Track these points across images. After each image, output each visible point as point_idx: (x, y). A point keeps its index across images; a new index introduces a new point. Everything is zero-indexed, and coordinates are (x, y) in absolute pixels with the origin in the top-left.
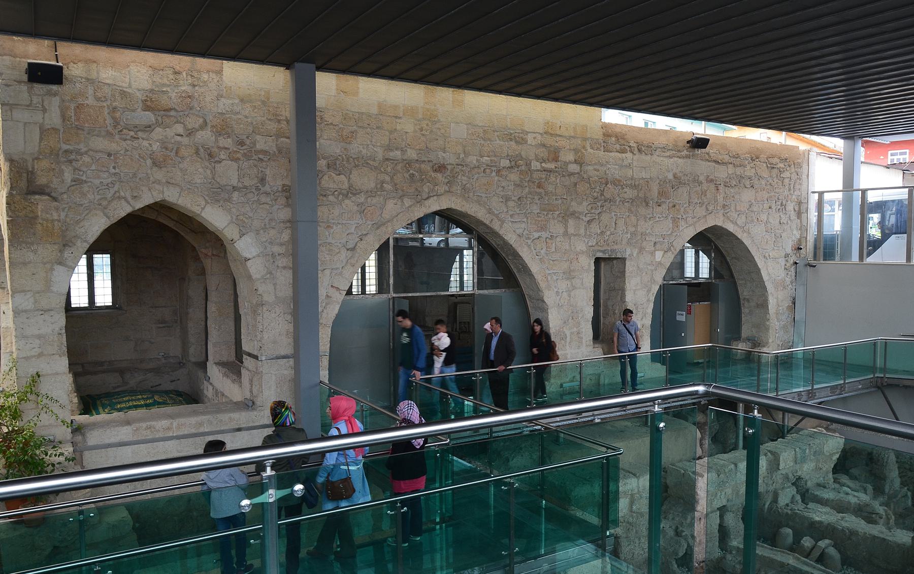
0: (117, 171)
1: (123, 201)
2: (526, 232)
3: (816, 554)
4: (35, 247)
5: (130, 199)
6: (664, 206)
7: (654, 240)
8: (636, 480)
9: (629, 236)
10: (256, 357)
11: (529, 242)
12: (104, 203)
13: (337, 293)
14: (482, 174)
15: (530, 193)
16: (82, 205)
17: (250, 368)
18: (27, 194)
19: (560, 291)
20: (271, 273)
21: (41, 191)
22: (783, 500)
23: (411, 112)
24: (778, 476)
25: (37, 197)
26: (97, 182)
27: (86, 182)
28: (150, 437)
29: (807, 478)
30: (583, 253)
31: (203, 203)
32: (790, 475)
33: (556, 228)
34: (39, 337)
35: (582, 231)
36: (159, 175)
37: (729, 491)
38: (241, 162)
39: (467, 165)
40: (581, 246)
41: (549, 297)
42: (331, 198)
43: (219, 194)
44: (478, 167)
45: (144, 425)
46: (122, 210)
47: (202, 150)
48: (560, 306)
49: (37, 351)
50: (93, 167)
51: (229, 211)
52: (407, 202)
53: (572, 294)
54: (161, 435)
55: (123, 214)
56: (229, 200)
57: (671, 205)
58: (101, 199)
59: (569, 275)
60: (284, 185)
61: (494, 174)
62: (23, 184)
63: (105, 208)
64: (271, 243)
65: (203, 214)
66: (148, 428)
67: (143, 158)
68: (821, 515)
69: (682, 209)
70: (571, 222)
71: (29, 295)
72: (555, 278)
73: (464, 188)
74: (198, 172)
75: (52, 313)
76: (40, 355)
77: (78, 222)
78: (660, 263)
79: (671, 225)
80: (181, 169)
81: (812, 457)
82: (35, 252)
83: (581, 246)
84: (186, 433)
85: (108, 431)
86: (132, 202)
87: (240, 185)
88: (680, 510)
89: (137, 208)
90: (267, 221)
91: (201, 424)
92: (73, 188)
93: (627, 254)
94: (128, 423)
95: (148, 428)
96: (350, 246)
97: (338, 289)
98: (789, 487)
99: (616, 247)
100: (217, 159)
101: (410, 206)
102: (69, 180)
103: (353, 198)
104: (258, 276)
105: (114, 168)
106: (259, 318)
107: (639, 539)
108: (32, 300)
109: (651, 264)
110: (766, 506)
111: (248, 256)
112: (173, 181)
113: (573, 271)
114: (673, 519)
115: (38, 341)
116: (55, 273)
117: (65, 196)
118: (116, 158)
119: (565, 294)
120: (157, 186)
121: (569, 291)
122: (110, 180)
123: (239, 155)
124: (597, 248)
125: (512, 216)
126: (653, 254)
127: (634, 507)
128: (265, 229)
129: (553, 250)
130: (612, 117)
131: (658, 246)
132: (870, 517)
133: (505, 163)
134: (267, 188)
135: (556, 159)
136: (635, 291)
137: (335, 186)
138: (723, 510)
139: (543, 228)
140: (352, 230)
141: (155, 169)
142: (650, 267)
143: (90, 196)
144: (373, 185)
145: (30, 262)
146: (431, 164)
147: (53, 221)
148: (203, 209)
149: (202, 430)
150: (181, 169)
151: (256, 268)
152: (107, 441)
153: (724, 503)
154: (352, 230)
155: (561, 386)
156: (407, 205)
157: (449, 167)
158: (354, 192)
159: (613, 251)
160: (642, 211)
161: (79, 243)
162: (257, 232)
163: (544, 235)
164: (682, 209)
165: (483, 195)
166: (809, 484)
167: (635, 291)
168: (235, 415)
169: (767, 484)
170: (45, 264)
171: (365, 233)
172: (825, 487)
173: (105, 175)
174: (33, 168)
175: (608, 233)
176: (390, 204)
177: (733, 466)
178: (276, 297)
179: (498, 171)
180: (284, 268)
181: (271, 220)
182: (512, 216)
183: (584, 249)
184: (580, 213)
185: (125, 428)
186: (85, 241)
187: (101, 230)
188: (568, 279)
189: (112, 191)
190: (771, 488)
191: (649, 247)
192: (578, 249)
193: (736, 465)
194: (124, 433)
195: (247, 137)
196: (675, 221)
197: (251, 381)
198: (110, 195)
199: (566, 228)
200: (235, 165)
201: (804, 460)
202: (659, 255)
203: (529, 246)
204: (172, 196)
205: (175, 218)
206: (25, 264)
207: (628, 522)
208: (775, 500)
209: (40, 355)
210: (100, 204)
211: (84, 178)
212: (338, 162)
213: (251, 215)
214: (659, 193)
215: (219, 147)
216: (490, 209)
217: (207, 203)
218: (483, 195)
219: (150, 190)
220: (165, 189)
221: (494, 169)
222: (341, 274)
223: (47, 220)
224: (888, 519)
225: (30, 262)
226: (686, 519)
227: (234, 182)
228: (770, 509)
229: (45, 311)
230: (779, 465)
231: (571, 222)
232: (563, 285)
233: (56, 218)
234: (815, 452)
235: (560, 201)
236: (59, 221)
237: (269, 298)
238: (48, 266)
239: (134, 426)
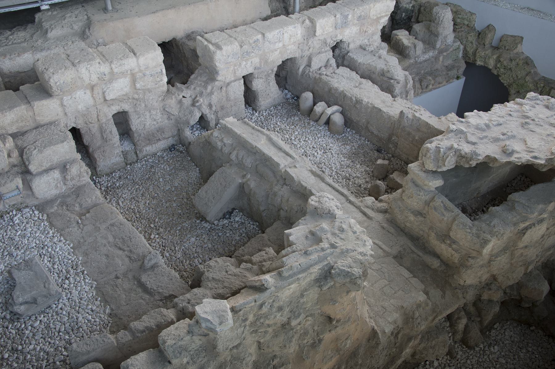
3: (324, 119)
8: (135, 59)
22: (316, 64)
24: (315, 43)
29: (349, 41)
32: (329, 41)
68: (344, 81)
81: (356, 22)
88: (205, 79)
107: (150, 112)
110: (301, 70)
114: (195, 89)
127: (138, 86)
132: (385, 83)
153: (250, 70)
166: (352, 46)
169: (302, 50)
172: (365, 49)
177: (260, 36)
190: (307, 53)
193: (263, 35)
201: (345, 24)
207: (134, 99)
208: (309, 65)
224: (407, 83)
226: (206, 89)
228: (304, 72)
230: (315, 31)
234: (360, 17)
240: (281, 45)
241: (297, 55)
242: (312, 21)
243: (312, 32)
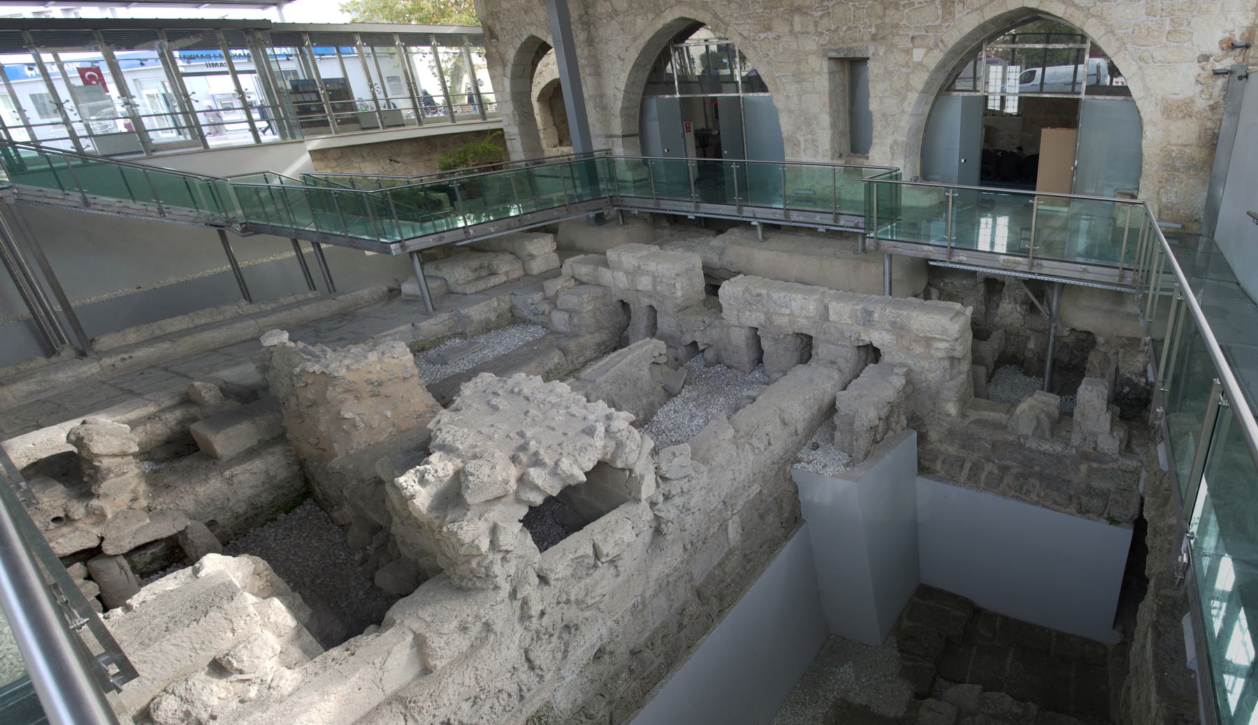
7: (911, 33)
9: (873, 30)
33: (780, 27)
35: (811, 28)
40: (811, 44)
59: (798, 78)
70: (797, 19)
78: (920, 64)
79: (940, 12)
83: (811, 44)
99: (854, 45)
109: (907, 65)
121: (799, 96)
126: (908, 52)
131: (917, 42)
139: (768, 28)
142: (904, 70)
159: (850, 49)
163: (771, 35)
175: (845, 28)
176: (639, 20)
183: (815, 47)
184: (810, 7)
188: (798, 82)
191: (904, 43)
192: (808, 48)
199: (792, 25)
202: (918, 55)
203: (755, 48)
231: (797, 19)
232: (792, 88)
240: (788, 312)
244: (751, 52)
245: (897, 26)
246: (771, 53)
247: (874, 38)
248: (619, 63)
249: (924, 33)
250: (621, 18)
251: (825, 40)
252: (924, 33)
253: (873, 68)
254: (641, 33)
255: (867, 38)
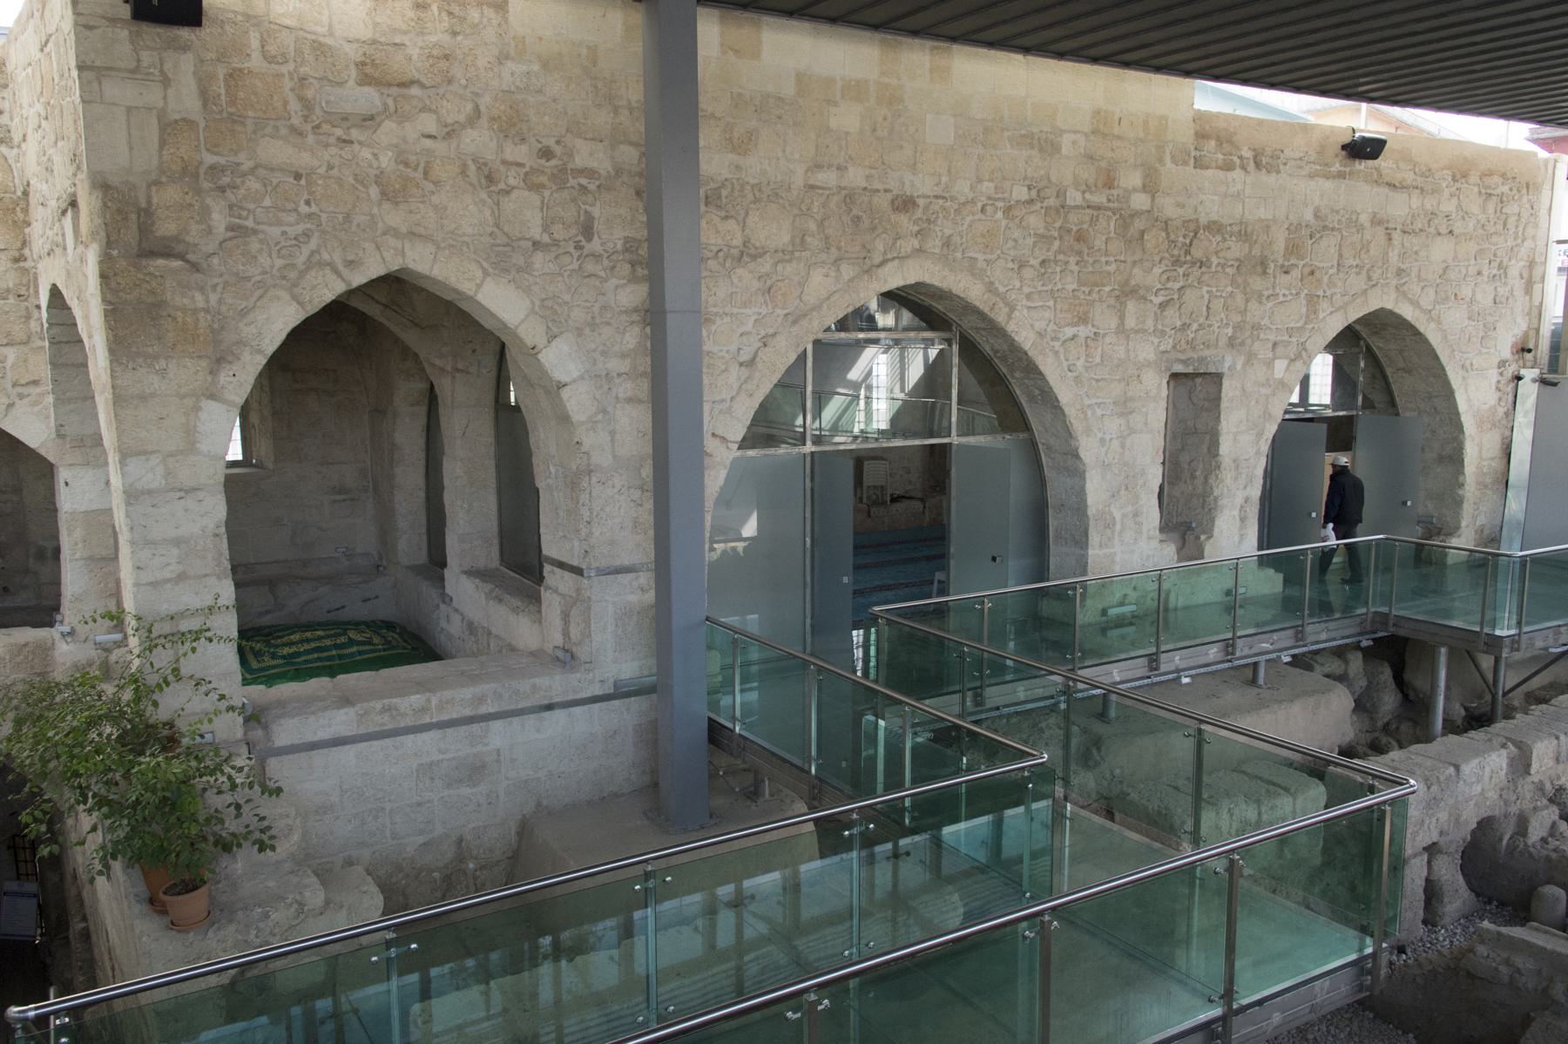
0: (314, 209)
1: (327, 270)
2: (1052, 326)
4: (163, 363)
5: (341, 268)
6: (1296, 273)
7: (1272, 337)
10: (578, 571)
11: (1057, 344)
12: (293, 275)
13: (723, 449)
14: (979, 216)
15: (1060, 251)
16: (248, 279)
17: (562, 589)
18: (138, 256)
19: (1108, 437)
20: (605, 411)
21: (166, 250)
22: (1537, 831)
23: (856, 90)
24: (1526, 788)
25: (161, 262)
26: (275, 232)
27: (255, 232)
28: (390, 726)
30: (1149, 365)
31: (479, 274)
32: (1548, 786)
33: (1105, 319)
34: (178, 542)
35: (1150, 323)
36: (394, 217)
37: (1443, 816)
38: (547, 193)
39: (953, 199)
41: (1089, 450)
42: (712, 264)
43: (504, 255)
44: (973, 201)
45: (378, 705)
46: (326, 290)
47: (473, 167)
48: (1106, 467)
49: (175, 569)
50: (267, 202)
51: (527, 291)
52: (847, 271)
53: (1128, 443)
54: (409, 722)
55: (329, 297)
56: (527, 268)
57: (1307, 270)
58: (286, 266)
59: (1124, 406)
60: (627, 240)
61: (1000, 215)
62: (131, 235)
63: (295, 285)
64: (604, 353)
65: (480, 297)
66: (385, 710)
67: (362, 183)
69: (1326, 279)
70: (1131, 306)
71: (155, 460)
72: (1099, 412)
73: (947, 243)
74: (468, 213)
75: (201, 495)
76: (181, 577)
77: (243, 313)
80: (435, 207)
82: (163, 373)
83: (1146, 351)
84: (455, 716)
85: (312, 718)
86: (345, 272)
87: (546, 239)
89: (355, 284)
90: (596, 310)
91: (481, 700)
92: (229, 244)
93: (1227, 365)
94: (346, 701)
95: (385, 710)
96: (745, 357)
97: (723, 439)
98: (1546, 807)
99: (1206, 353)
100: (502, 186)
101: (852, 280)
102: (222, 229)
103: (752, 266)
104: (583, 418)
105: (308, 203)
106: (584, 497)
108: (160, 470)
111: (564, 378)
112: (421, 231)
113: (1132, 399)
115: (175, 551)
116: (203, 415)
117: (215, 261)
118: (309, 184)
119: (1116, 443)
120: (392, 242)
122: (300, 228)
123: (543, 179)
124: (1174, 355)
125: (1028, 296)
126: (1270, 364)
128: (593, 326)
129: (1098, 360)
130: (1215, 99)
131: (1279, 350)
133: (1020, 193)
134: (596, 245)
135: (1109, 184)
136: (1236, 435)
137: (720, 241)
138: (1432, 850)
139: (1083, 320)
140: (749, 327)
141: (386, 206)
142: (1264, 391)
143: (264, 260)
144: (786, 239)
145: (153, 395)
146: (889, 196)
147: (195, 311)
148: (479, 286)
149: (483, 710)
150: (435, 207)
151: (578, 402)
152: (310, 738)
153: (1435, 837)
154: (749, 327)
155: (1104, 612)
156: (846, 278)
157: (921, 202)
158: (752, 251)
159: (1202, 360)
160: (1257, 283)
161: (246, 356)
162: (579, 332)
163: (1083, 331)
164: (1326, 279)
165: (980, 257)
167: (1236, 435)
168: (542, 681)
169: (1506, 803)
170: (182, 397)
171: (771, 331)
173: (292, 218)
174: (149, 202)
175: (1195, 326)
177: (1452, 769)
178: (615, 457)
179: (1008, 210)
180: (629, 400)
181: (604, 308)
182: (1028, 296)
183: (1152, 357)
184: (1148, 289)
185: (342, 711)
186: (260, 352)
187: (289, 329)
188: (1121, 415)
189: (306, 251)
190: (1514, 809)
191: (1264, 352)
192: (1141, 358)
193: (1457, 768)
194: (341, 721)
195: (558, 142)
196: (1312, 300)
197: (566, 617)
198: (303, 258)
199: (1122, 318)
200: (535, 199)
204: (420, 260)
205: (383, 300)
206: (143, 398)
209: (181, 577)
210: (284, 278)
211: (250, 223)
212: (724, 193)
213: (567, 297)
214: (1287, 248)
215: (504, 162)
216: (992, 283)
217: (486, 273)
218: (980, 257)
219: (378, 248)
220: (407, 246)
221: (1000, 204)
222: (729, 411)
223: (184, 310)
225: (153, 395)
227: (536, 232)
228: (1512, 848)
229: (187, 492)
230: (1529, 765)
231: (1131, 306)
232: (1113, 426)
233: (201, 304)
235: (1112, 268)
236: (207, 311)
237: (602, 459)
238: (189, 402)
239: (359, 708)
240: (1479, 789)
241: (1497, 813)
242: (1519, 745)
243: (1521, 764)
244: (1050, 360)
245: (1256, 327)
246: (1080, 364)
247: (1231, 343)
248: (735, 374)
249: (1286, 338)
250: (766, 265)
251: (1167, 344)
252: (1286, 338)
253: (1229, 388)
254: (817, 308)
255: (1223, 341)
